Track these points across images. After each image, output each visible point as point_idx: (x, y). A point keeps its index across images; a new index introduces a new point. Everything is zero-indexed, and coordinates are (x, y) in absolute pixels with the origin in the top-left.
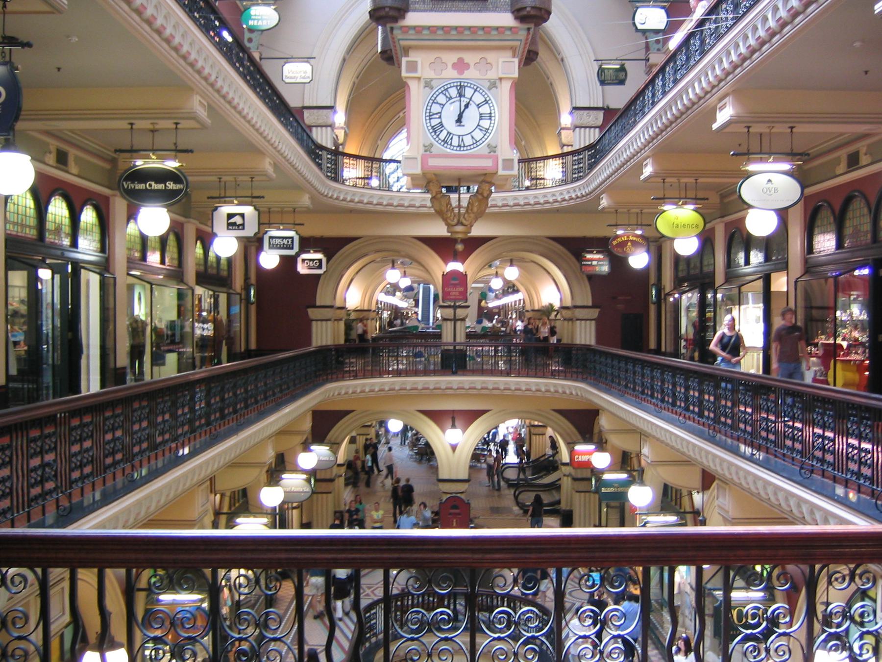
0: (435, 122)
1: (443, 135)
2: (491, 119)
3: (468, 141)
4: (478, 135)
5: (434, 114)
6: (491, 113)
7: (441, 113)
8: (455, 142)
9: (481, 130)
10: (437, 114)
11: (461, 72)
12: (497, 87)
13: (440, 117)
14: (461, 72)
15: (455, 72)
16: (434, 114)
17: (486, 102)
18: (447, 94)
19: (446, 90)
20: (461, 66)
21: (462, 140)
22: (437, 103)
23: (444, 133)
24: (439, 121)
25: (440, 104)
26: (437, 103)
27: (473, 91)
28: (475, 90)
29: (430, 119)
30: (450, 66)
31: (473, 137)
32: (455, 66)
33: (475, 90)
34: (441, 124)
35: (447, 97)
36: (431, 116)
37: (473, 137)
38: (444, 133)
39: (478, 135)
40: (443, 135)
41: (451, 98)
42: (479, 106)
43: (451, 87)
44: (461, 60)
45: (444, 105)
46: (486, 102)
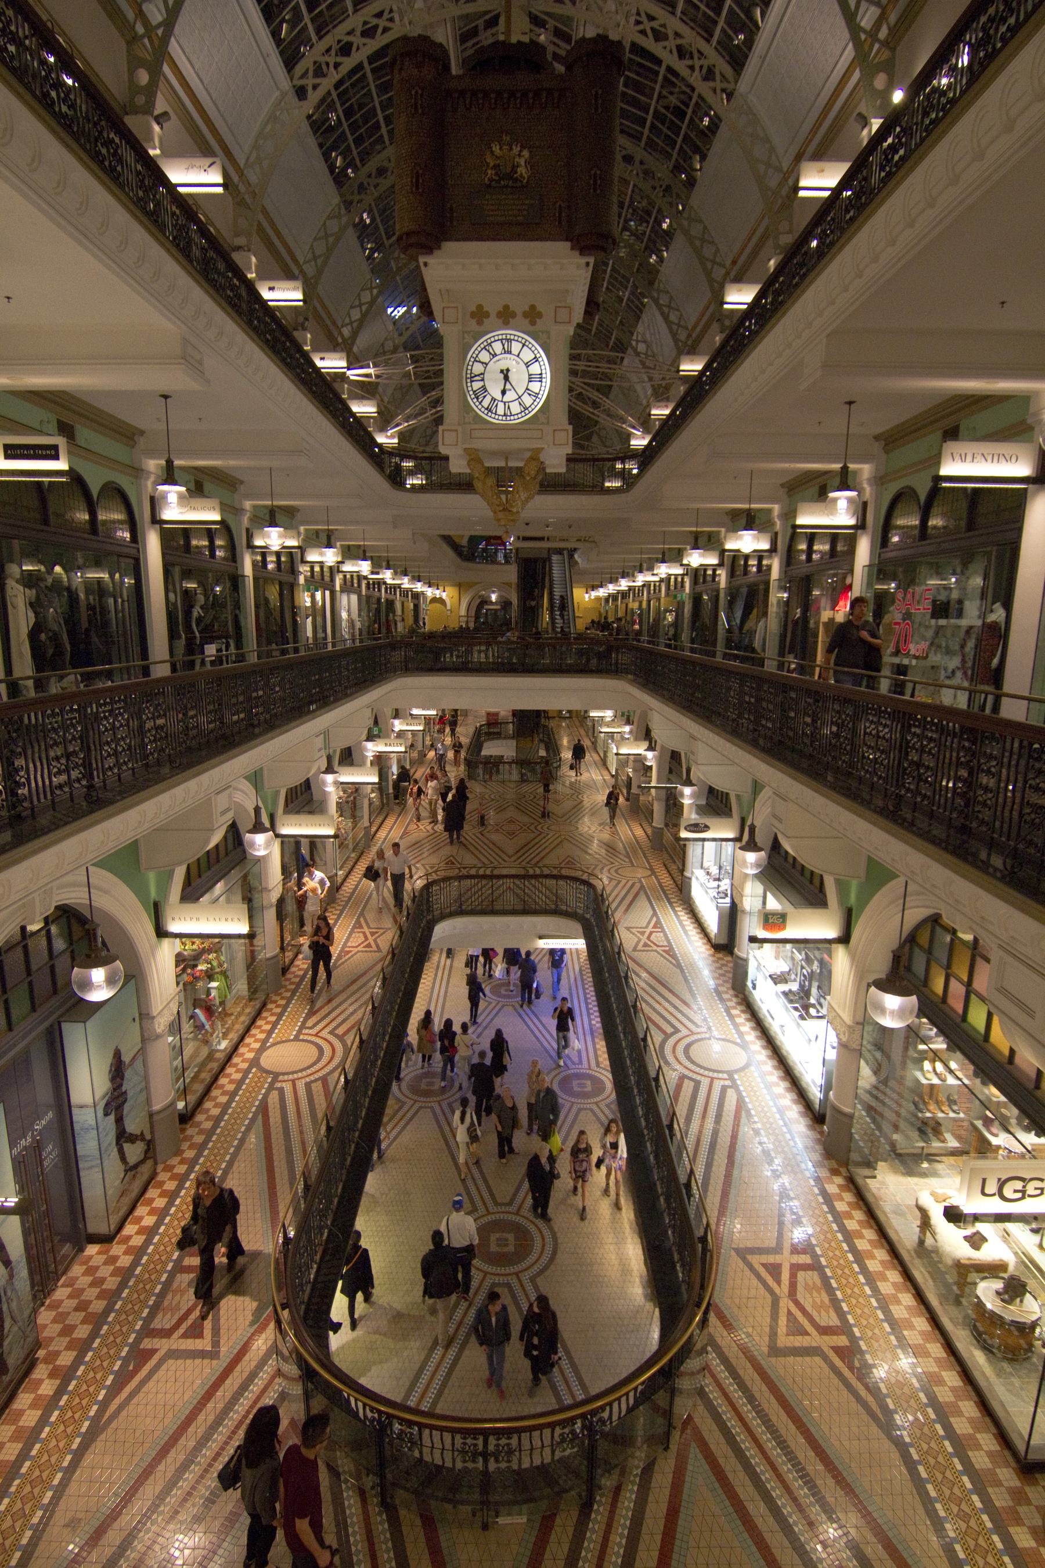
0: (477, 385)
8: (501, 410)
19: (490, 345)
23: (488, 400)
24: (481, 384)
30: (493, 315)
34: (484, 389)
38: (488, 400)
42: (527, 365)
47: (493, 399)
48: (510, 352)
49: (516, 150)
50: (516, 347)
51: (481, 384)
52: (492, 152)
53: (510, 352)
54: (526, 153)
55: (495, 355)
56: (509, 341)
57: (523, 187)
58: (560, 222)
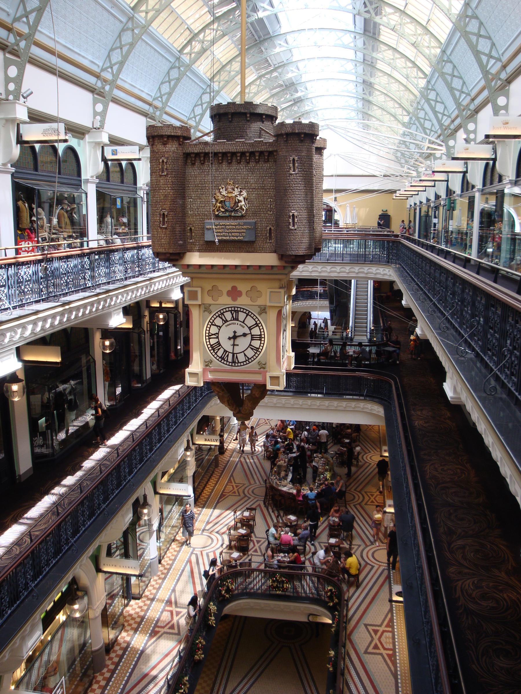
0: (213, 341)
1: (220, 353)
2: (261, 340)
3: (241, 358)
4: (250, 353)
5: (212, 335)
6: (261, 335)
7: (218, 334)
9: (252, 349)
10: (214, 334)
11: (235, 299)
12: (266, 313)
13: (218, 338)
14: (235, 299)
15: (230, 298)
16: (212, 335)
17: (257, 325)
18: (223, 318)
19: (222, 314)
20: (234, 293)
21: (237, 357)
22: (215, 325)
24: (217, 340)
25: (217, 326)
26: (215, 325)
27: (245, 315)
28: (247, 315)
29: (209, 339)
30: (225, 293)
31: (245, 355)
32: (229, 293)
33: (247, 315)
34: (219, 343)
35: (223, 320)
36: (210, 336)
37: (245, 355)
39: (250, 353)
40: (220, 353)
41: (226, 321)
43: (226, 311)
44: (234, 288)
45: (220, 327)
46: (257, 325)
47: (225, 351)
48: (237, 319)
49: (236, 192)
50: (242, 316)
51: (217, 340)
52: (220, 192)
53: (237, 319)
54: (245, 193)
55: (226, 321)
56: (237, 312)
57: (242, 217)
58: (270, 238)
